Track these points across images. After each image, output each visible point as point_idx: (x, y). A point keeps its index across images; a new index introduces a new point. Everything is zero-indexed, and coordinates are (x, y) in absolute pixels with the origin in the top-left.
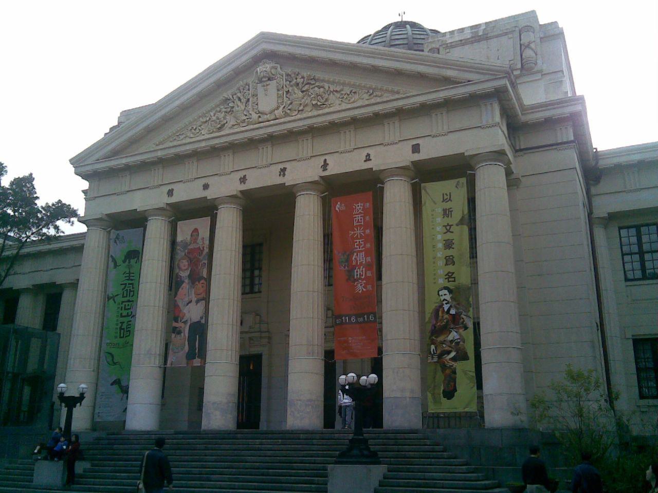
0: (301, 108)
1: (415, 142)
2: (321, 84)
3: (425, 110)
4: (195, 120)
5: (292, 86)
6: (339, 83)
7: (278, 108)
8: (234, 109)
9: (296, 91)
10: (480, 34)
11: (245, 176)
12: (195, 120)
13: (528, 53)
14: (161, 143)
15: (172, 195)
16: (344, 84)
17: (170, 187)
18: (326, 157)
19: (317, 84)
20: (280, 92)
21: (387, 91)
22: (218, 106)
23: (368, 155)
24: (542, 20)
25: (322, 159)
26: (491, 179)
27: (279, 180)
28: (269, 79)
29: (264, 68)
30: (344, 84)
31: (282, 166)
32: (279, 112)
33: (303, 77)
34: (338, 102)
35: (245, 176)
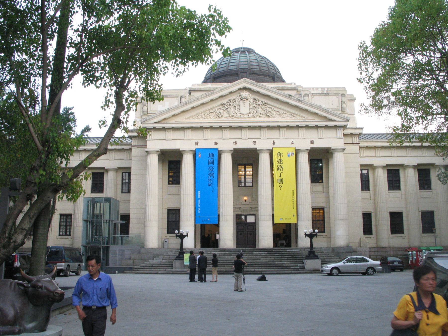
0: (261, 115)
1: (312, 140)
2: (270, 107)
3: (317, 127)
4: (207, 110)
5: (256, 104)
6: (278, 108)
7: (250, 113)
8: (228, 110)
9: (260, 108)
10: (325, 92)
11: (236, 142)
12: (207, 110)
13: (344, 105)
14: (188, 118)
15: (198, 145)
16: (280, 109)
17: (197, 141)
18: (274, 140)
19: (268, 106)
20: (251, 106)
21: (299, 116)
22: (218, 106)
23: (293, 142)
24: (349, 92)
25: (273, 140)
26: (338, 158)
27: (253, 146)
28: (246, 99)
29: (245, 94)
30: (280, 109)
31: (254, 140)
32: (251, 115)
33: (262, 102)
34: (277, 116)
35: (236, 142)
